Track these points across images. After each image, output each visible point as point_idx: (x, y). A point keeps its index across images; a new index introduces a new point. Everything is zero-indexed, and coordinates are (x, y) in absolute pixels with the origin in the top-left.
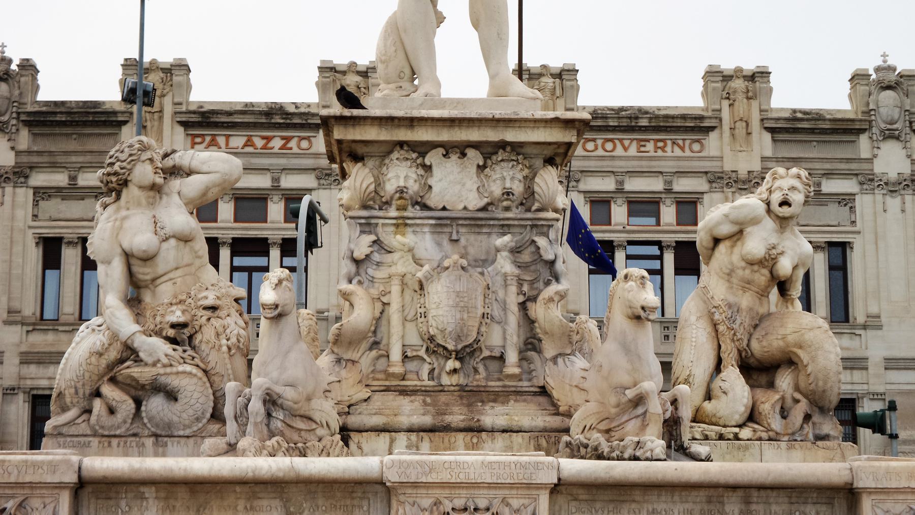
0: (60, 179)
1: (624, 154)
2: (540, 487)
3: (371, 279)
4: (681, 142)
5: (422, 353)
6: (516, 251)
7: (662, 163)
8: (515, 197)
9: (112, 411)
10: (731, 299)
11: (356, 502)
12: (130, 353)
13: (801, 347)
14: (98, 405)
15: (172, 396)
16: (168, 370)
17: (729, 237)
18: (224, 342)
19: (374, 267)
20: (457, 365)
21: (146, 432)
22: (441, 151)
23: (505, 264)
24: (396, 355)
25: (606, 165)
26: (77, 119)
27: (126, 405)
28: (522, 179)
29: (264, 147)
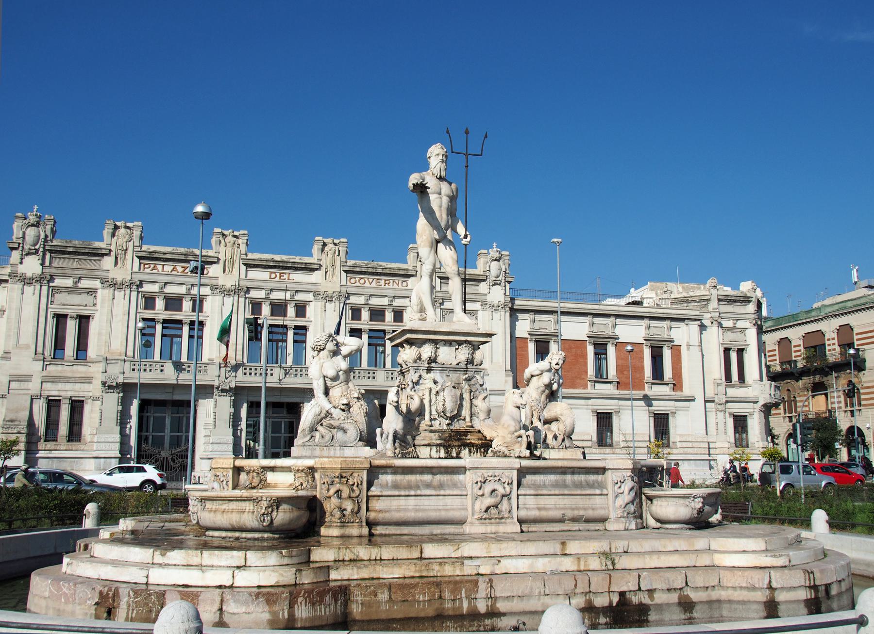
0: (69, 282)
1: (370, 286)
4: (397, 281)
7: (387, 291)
13: (562, 415)
14: (317, 435)
15: (345, 431)
16: (344, 422)
18: (362, 411)
22: (443, 342)
25: (360, 291)
26: (79, 251)
29: (183, 272)
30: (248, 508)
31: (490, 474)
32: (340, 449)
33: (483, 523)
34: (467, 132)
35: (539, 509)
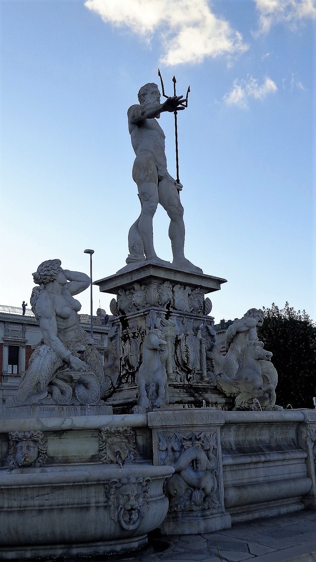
9: (63, 392)
12: (66, 363)
15: (86, 386)
16: (86, 373)
17: (244, 332)
21: (78, 403)
27: (69, 390)
30: (93, 500)
32: (81, 409)
34: (174, 80)
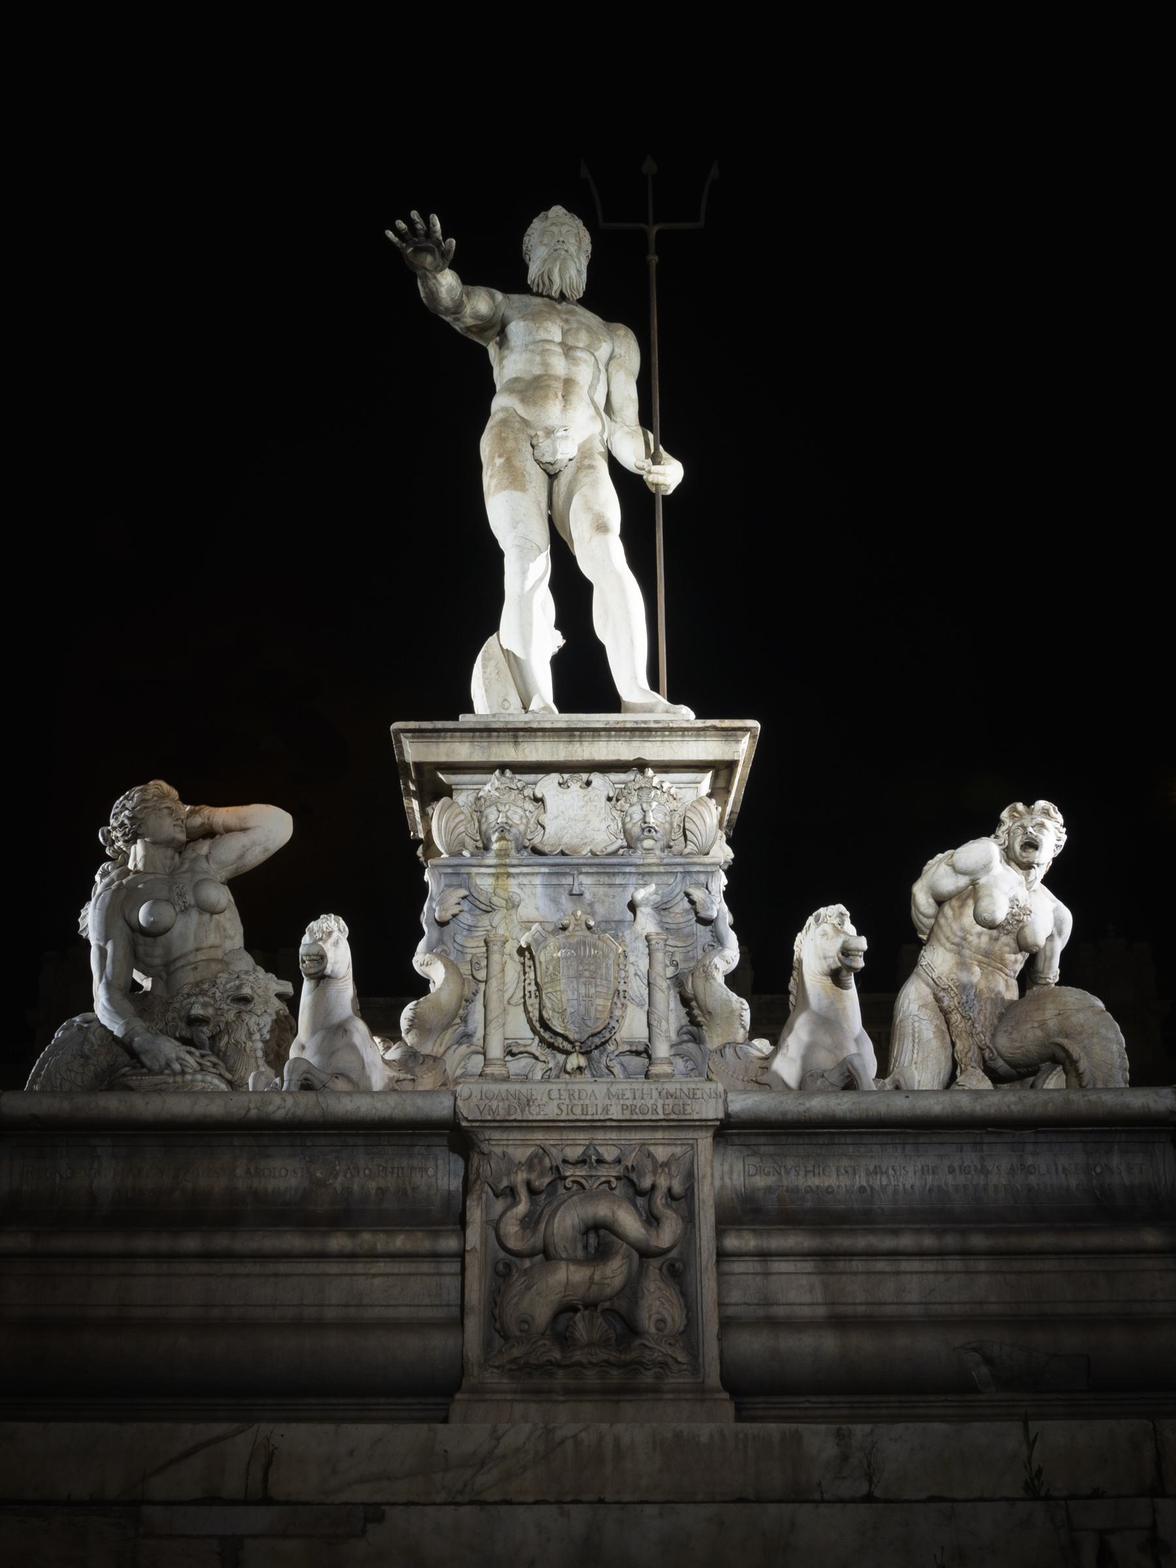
2: (700, 1125)
3: (460, 949)
5: (535, 1048)
6: (661, 908)
8: (659, 835)
10: (964, 977)
11: (415, 1163)
13: (1067, 1036)
19: (465, 933)
20: (583, 1061)
22: (555, 777)
23: (646, 923)
24: (496, 1050)
28: (668, 813)
31: (574, 1153)
33: (538, 1391)
35: (839, 1322)
